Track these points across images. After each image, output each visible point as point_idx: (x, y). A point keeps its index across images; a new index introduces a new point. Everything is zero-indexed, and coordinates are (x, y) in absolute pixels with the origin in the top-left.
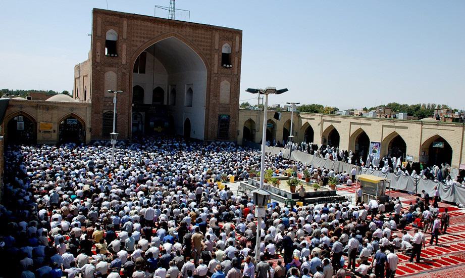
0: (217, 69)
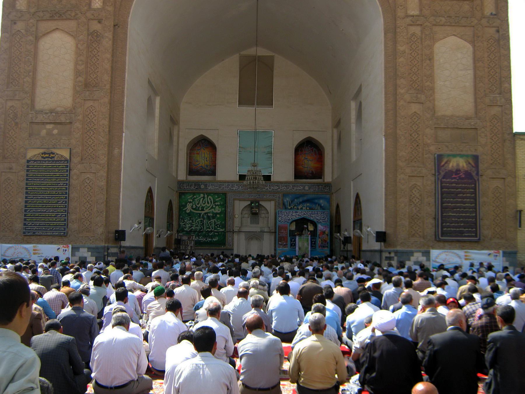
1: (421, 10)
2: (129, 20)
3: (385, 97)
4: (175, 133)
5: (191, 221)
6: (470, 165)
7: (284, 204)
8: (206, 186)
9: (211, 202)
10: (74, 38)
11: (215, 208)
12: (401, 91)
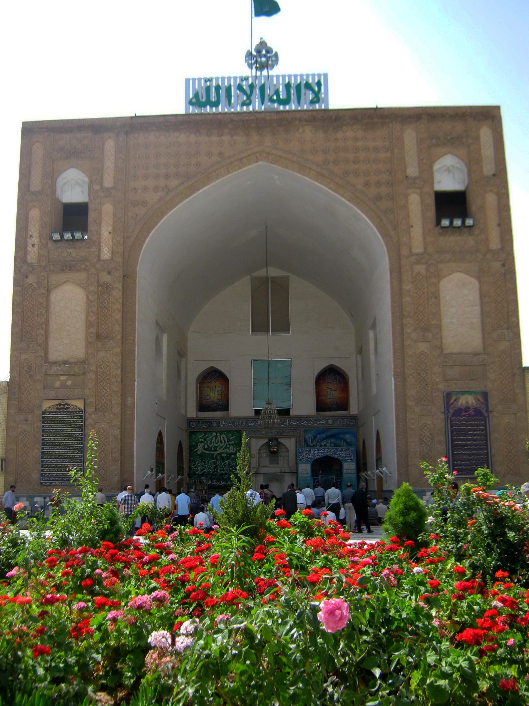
0: (421, 239)
1: (425, 248)
2: (138, 269)
3: (393, 336)
4: (183, 366)
5: (203, 464)
6: (479, 402)
8: (218, 423)
9: (225, 441)
10: (85, 289)
11: (229, 448)
12: (408, 330)
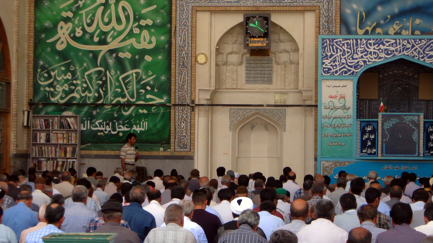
5: (69, 76)
7: (344, 22)
9: (127, 18)
11: (137, 36)
